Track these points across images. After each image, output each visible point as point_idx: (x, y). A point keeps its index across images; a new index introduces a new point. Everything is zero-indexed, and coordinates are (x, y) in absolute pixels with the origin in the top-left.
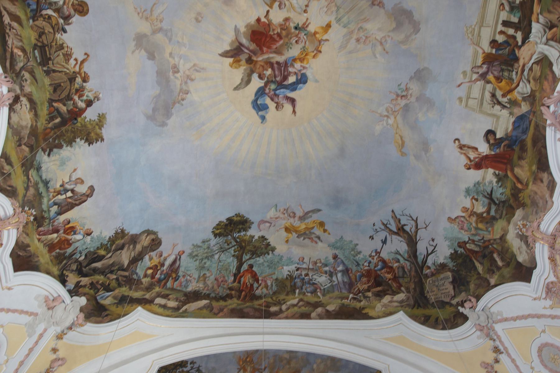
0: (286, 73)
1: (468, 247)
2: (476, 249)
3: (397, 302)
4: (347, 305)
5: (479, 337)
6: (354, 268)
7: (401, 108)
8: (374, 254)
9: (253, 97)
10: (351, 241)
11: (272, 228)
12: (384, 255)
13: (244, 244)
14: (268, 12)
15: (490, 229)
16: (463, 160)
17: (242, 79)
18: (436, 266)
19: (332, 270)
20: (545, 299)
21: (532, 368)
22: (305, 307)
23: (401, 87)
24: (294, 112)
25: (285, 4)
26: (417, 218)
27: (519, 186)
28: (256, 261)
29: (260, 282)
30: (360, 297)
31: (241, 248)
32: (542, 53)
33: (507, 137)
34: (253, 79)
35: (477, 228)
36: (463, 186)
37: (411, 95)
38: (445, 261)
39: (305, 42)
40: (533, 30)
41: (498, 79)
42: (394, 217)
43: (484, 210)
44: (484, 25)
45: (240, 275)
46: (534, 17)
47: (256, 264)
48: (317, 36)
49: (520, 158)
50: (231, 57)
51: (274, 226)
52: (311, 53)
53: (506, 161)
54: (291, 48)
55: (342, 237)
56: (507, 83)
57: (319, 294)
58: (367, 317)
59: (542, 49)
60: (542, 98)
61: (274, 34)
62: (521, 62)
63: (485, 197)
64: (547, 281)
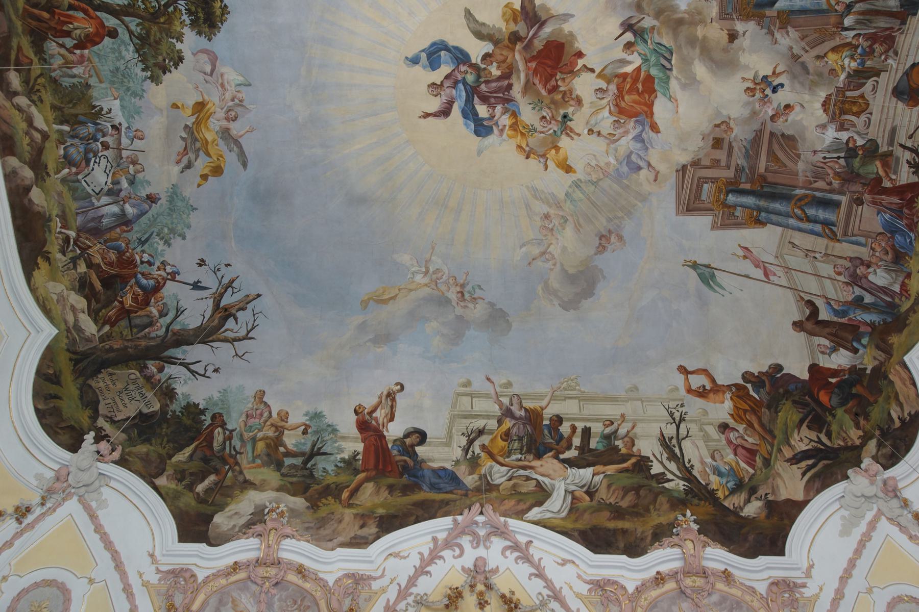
0: (493, 100)
1: (216, 431)
2: (215, 444)
3: (76, 320)
4: (49, 227)
5: (39, 477)
6: (133, 236)
7: (443, 293)
8: (169, 269)
9: (452, 42)
10: (189, 227)
11: (201, 77)
12: (170, 288)
13: (162, 20)
14: (592, 70)
15: (259, 461)
16: (369, 402)
17: (484, 24)
18: (166, 381)
19: (123, 194)
20: (158, 571)
22: (28, 145)
23: (477, 290)
24: (427, 115)
25: (603, 98)
26: (253, 338)
27: (345, 495)
28: (126, 45)
29: (78, 52)
30: (73, 251)
31: (152, 14)
32: (554, 490)
33: (419, 463)
34: (484, 43)
36: (323, 407)
37: (466, 307)
38: (181, 396)
39: (542, 132)
40: (582, 471)
41: (507, 435)
42: (248, 300)
43: (290, 447)
44: (581, 403)
45: (90, 10)
46: (599, 468)
47: (120, 46)
48: (553, 151)
49: (391, 488)
50: (523, 7)
51: (207, 82)
52: (525, 143)
53: (381, 467)
54: (534, 108)
55: (196, 209)
56: (503, 448)
57: (66, 171)
58: (29, 267)
59: (559, 488)
60: (489, 501)
61: (557, 81)
62: (536, 463)
63: (314, 446)
64: (193, 568)
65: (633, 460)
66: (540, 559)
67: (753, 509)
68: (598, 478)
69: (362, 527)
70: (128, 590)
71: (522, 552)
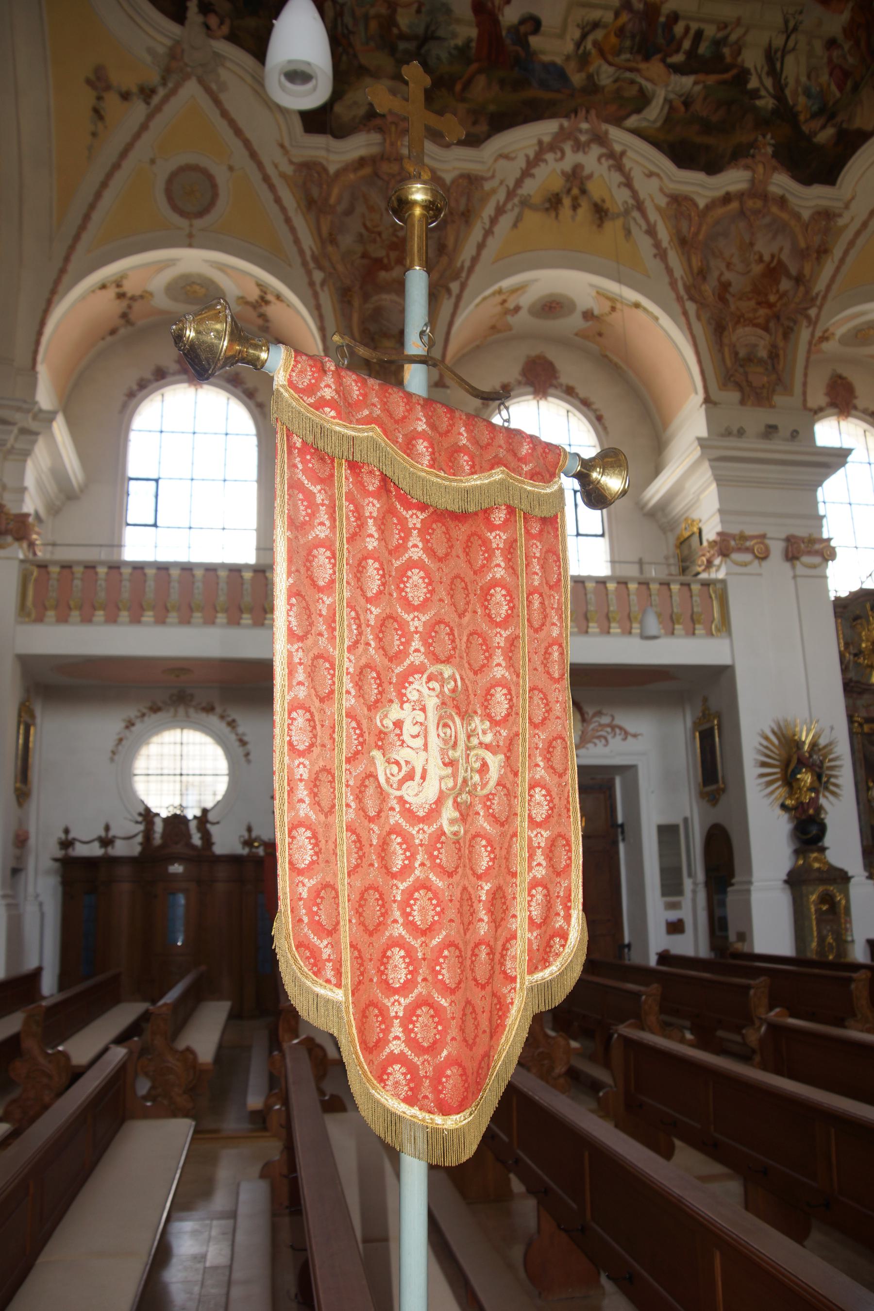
5: (150, 51)
20: (291, 162)
21: (153, 161)
27: (458, 87)
33: (531, 54)
35: (366, 18)
41: (621, 32)
43: (404, 28)
46: (701, 77)
62: (643, 66)
63: (427, 27)
65: (734, 72)
66: (631, 169)
67: (825, 136)
68: (698, 88)
69: (475, 123)
70: (266, 179)
71: (616, 160)
